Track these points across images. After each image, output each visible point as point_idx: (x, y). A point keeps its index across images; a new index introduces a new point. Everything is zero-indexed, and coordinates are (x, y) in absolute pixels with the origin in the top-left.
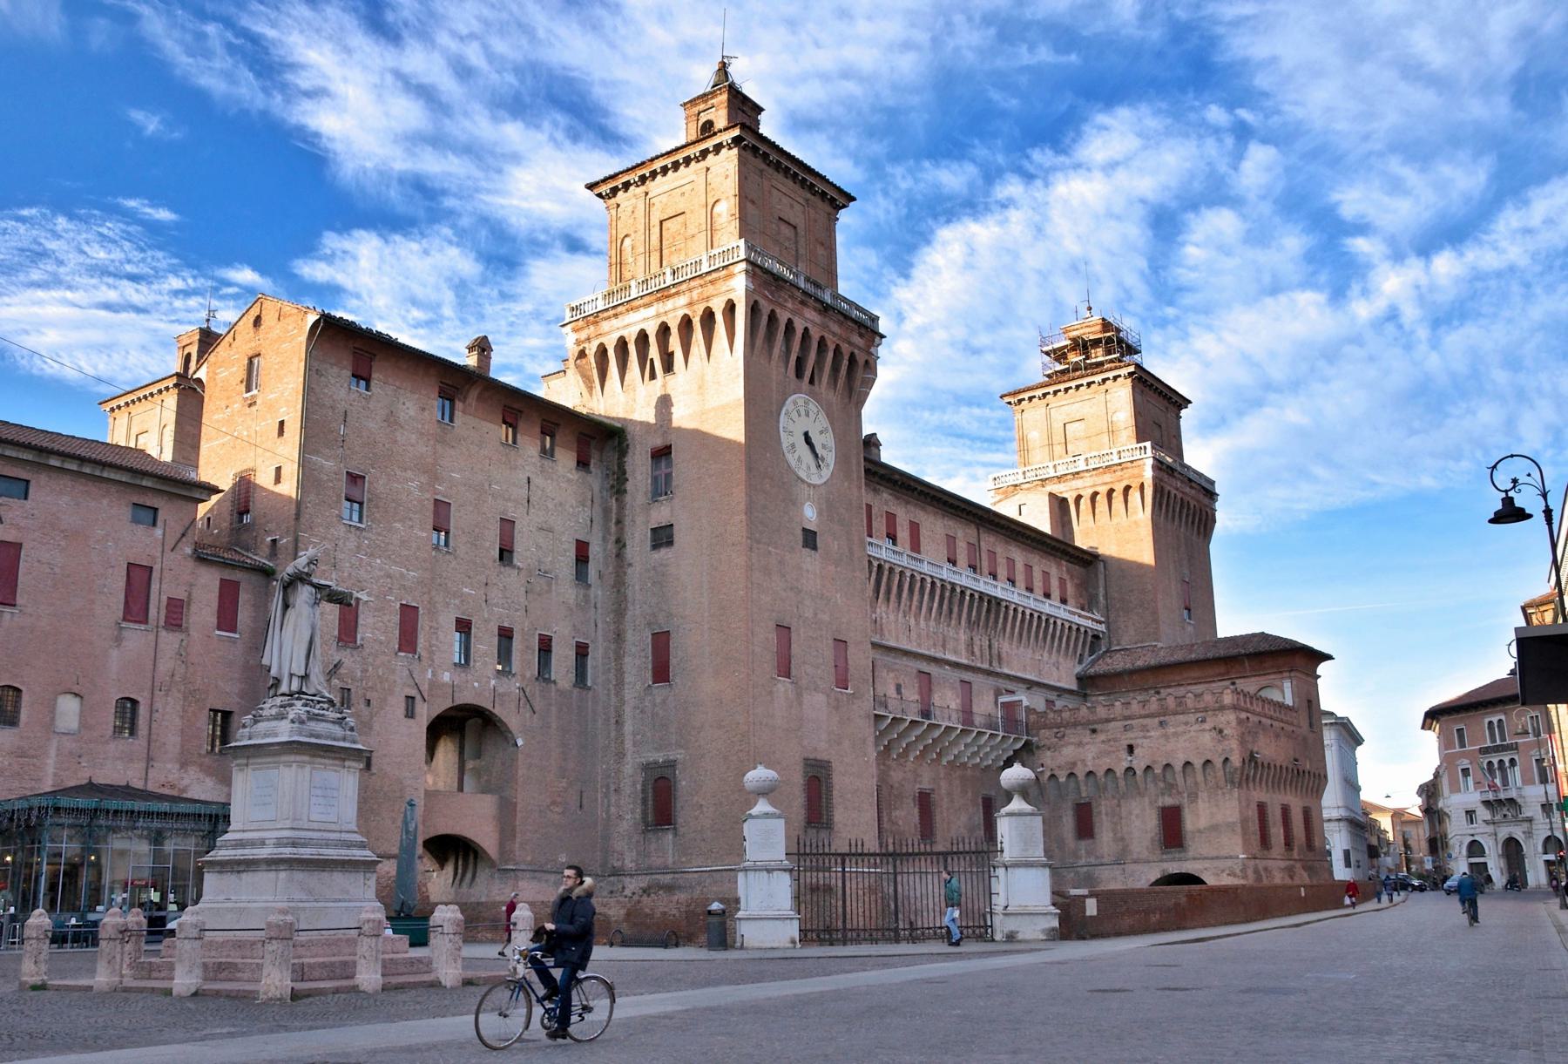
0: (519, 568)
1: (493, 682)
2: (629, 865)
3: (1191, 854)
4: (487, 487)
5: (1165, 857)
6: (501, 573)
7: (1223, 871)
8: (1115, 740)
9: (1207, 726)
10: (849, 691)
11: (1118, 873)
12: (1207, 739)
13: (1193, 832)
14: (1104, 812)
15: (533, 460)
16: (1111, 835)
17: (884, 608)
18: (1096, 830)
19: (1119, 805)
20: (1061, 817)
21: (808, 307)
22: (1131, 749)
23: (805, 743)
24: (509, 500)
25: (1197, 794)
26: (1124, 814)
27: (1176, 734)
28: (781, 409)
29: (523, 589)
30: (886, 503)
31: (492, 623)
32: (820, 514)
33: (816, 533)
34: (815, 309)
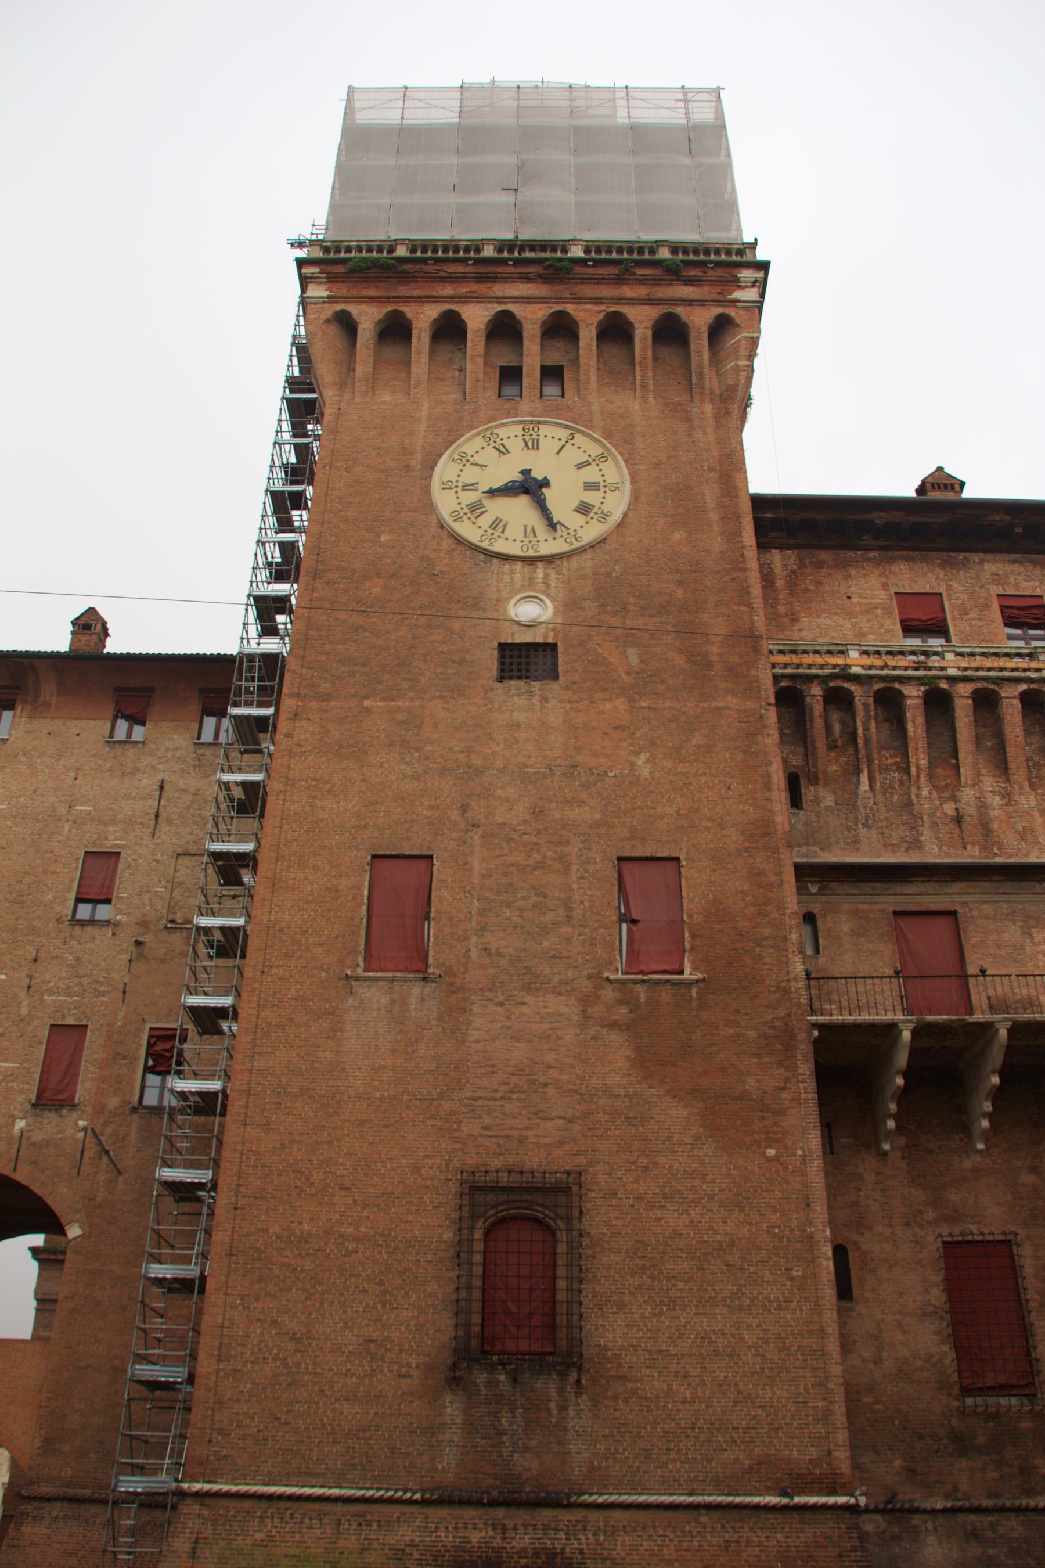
0: (117, 924)
4: (62, 810)
6: (72, 937)
10: (686, 975)
15: (178, 754)
17: (988, 783)
21: (506, 279)
23: (470, 1127)
24: (113, 821)
28: (440, 456)
29: (126, 957)
30: (997, 579)
31: (36, 1023)
32: (569, 605)
33: (553, 647)
34: (526, 279)
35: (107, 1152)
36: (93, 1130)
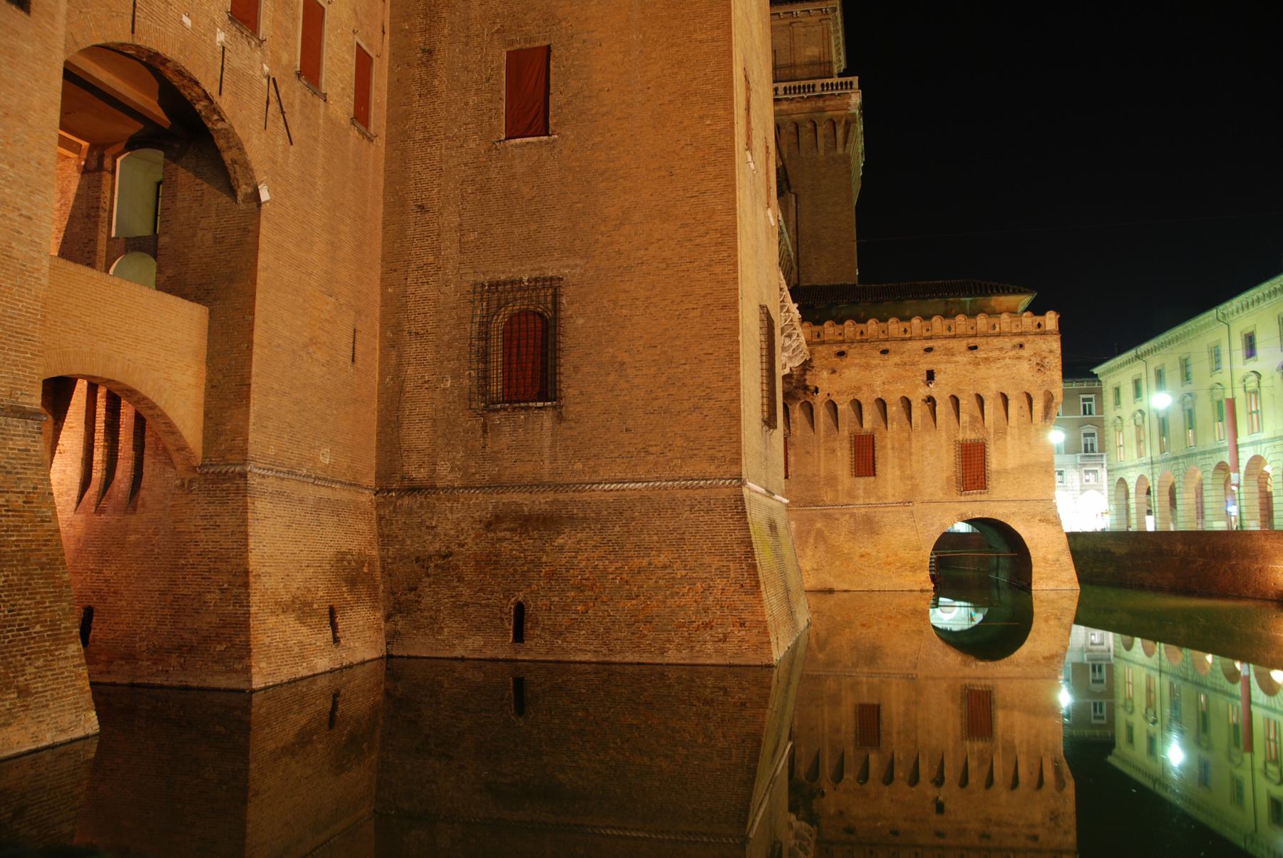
1: (221, 37)
2: (445, 473)
3: (994, 497)
5: (963, 498)
7: (1033, 516)
8: (913, 364)
9: (1023, 353)
11: (904, 516)
12: (1024, 367)
13: (998, 472)
14: (889, 446)
16: (898, 473)
18: (879, 467)
19: (909, 439)
20: (834, 451)
22: (930, 376)
25: (1006, 429)
26: (913, 450)
27: (986, 359)
35: (283, 113)
36: (274, 79)
